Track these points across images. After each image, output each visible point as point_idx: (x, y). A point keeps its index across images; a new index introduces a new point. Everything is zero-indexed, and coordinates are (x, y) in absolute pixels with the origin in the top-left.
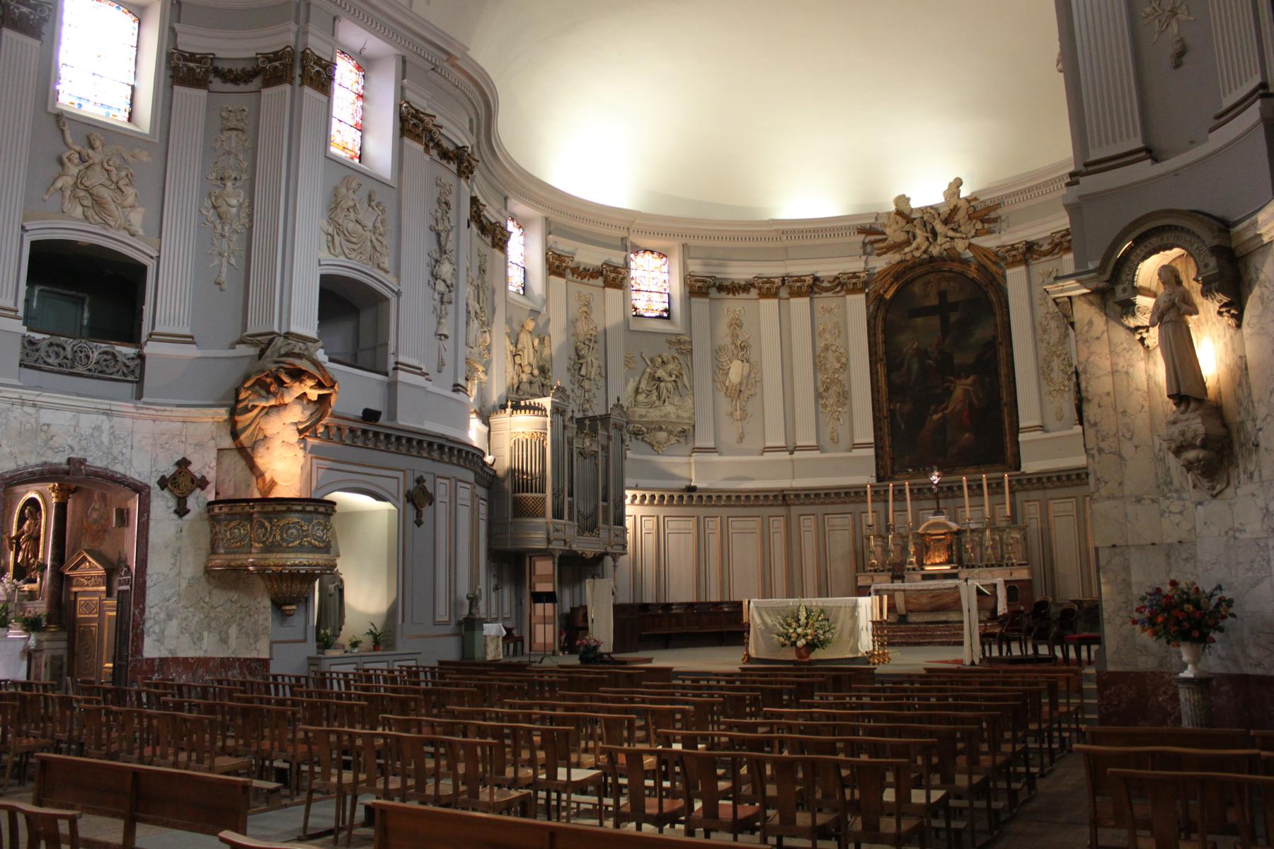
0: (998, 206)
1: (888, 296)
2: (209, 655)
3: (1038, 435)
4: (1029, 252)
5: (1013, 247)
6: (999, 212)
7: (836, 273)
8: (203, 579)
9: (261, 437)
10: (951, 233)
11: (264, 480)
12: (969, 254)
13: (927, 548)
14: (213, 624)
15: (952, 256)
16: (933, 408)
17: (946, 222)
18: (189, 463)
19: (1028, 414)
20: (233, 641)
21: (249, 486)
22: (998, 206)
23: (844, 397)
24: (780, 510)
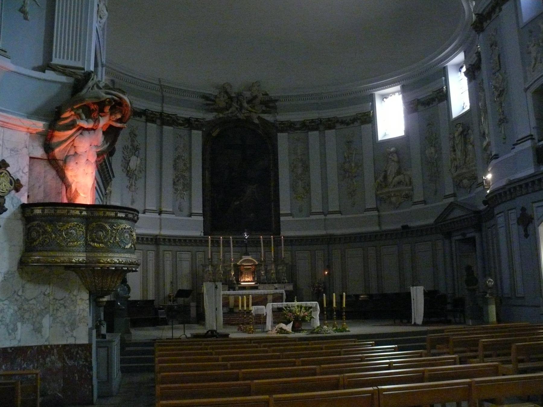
0: (276, 101)
1: (214, 134)
2: (22, 344)
3: (290, 218)
4: (289, 127)
5: (282, 123)
6: (277, 104)
7: (188, 117)
8: (17, 274)
9: (72, 152)
10: (250, 109)
11: (71, 189)
12: (256, 121)
13: (242, 273)
14: (27, 316)
15: (248, 120)
17: (249, 102)
18: (8, 165)
19: (284, 208)
20: (46, 332)
21: (59, 193)
22: (276, 101)
23: (188, 186)
24: (152, 247)
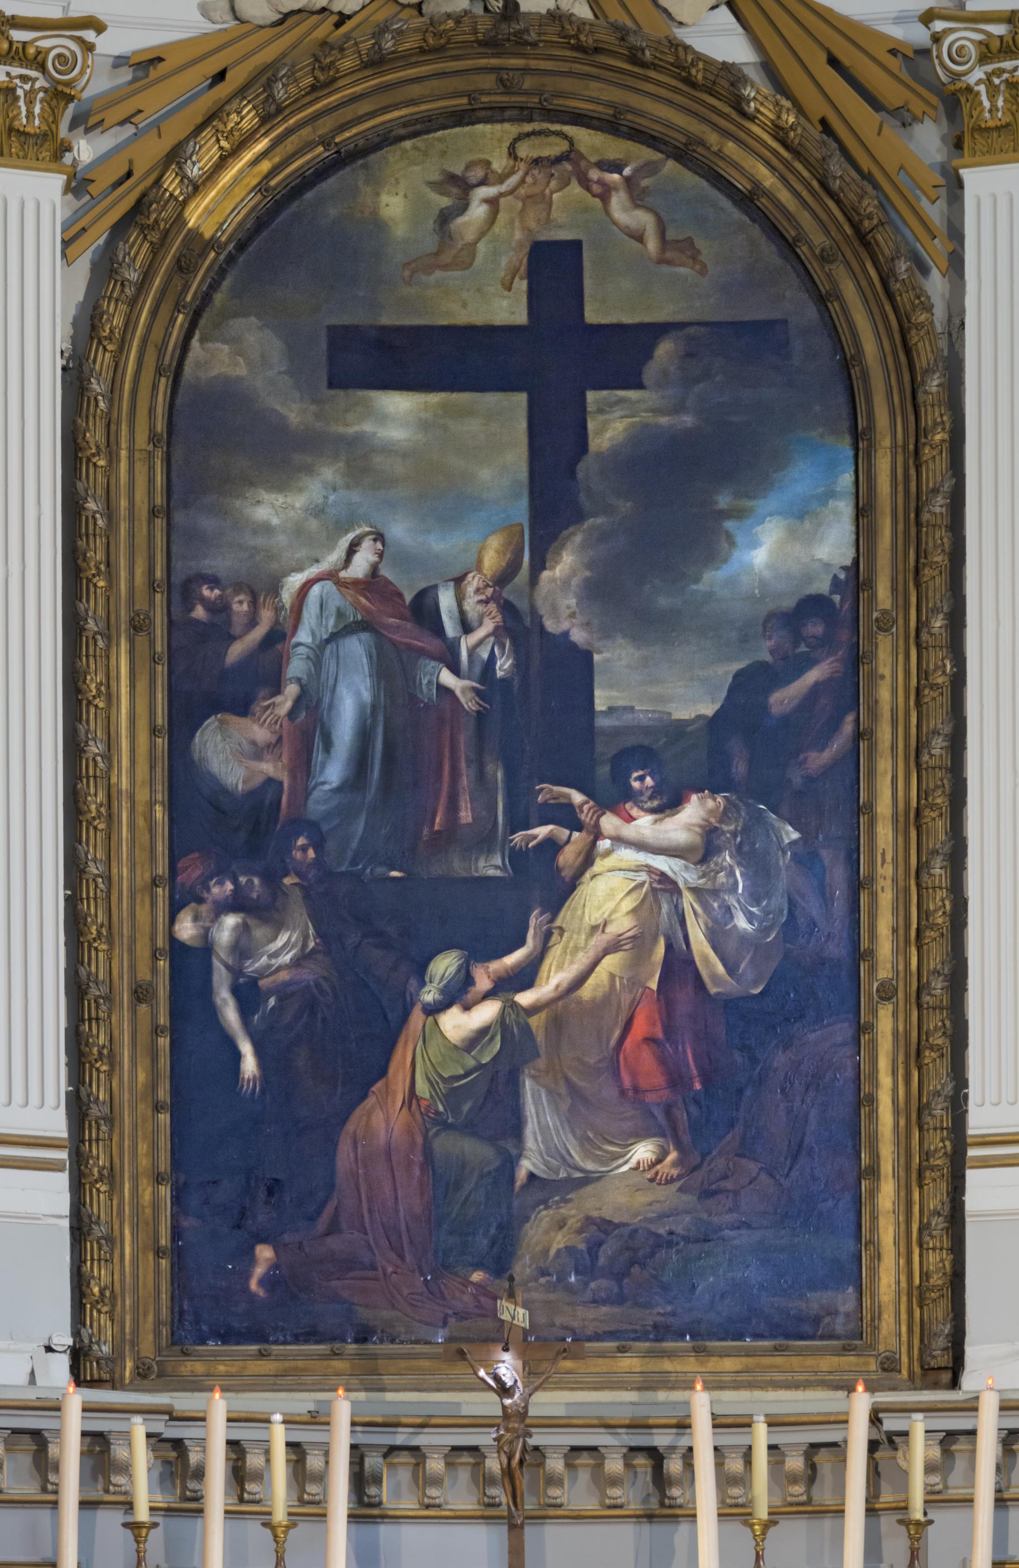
1: (214, 209)
16: (445, 965)
